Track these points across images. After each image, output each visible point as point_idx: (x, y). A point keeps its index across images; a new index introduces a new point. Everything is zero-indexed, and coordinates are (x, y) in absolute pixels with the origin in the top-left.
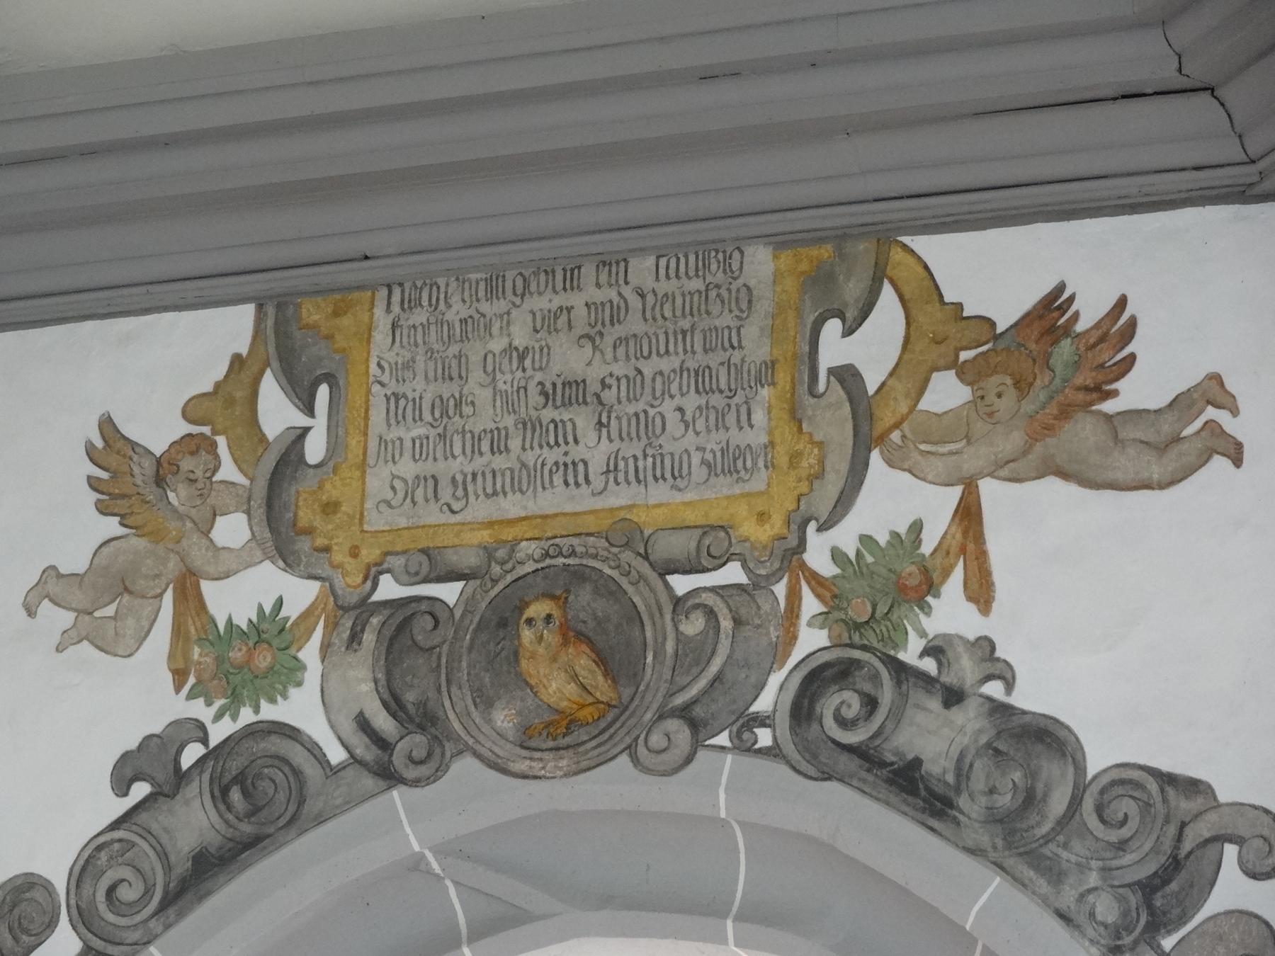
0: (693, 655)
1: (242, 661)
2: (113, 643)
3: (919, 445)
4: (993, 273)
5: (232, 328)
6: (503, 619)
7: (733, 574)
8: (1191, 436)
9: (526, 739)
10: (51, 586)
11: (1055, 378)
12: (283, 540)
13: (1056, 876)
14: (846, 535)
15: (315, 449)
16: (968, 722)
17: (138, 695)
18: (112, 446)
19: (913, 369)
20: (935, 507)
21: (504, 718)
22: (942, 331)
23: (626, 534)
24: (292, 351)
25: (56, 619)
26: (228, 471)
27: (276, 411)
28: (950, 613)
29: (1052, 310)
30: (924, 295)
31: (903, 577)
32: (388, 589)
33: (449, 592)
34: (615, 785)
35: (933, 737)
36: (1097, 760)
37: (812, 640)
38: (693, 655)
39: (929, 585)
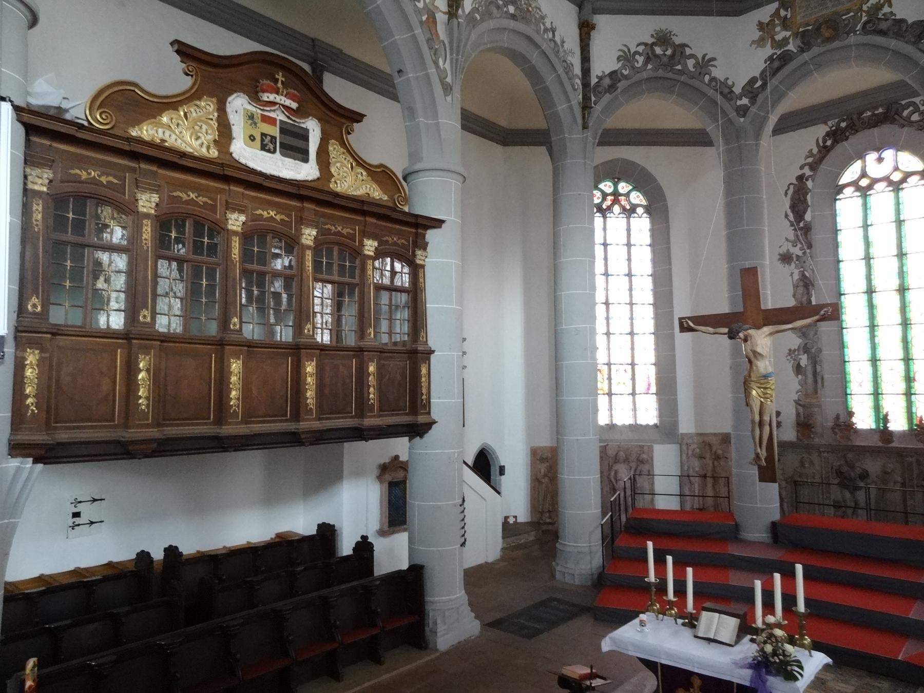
0: (846, 25)
2: (763, 46)
5: (776, 5)
6: (818, 29)
7: (852, 14)
9: (823, 42)
10: (753, 42)
12: (785, 27)
13: (904, 37)
14: (869, 4)
15: (789, 16)
16: (889, 23)
17: (768, 51)
21: (819, 41)
23: (835, 13)
24: (784, 5)
25: (754, 46)
26: (777, 22)
27: (783, 13)
28: (886, 9)
32: (801, 30)
33: (810, 28)
34: (837, 44)
35: (884, 26)
36: (910, 21)
37: (864, 19)
38: (846, 25)
39: (882, 6)
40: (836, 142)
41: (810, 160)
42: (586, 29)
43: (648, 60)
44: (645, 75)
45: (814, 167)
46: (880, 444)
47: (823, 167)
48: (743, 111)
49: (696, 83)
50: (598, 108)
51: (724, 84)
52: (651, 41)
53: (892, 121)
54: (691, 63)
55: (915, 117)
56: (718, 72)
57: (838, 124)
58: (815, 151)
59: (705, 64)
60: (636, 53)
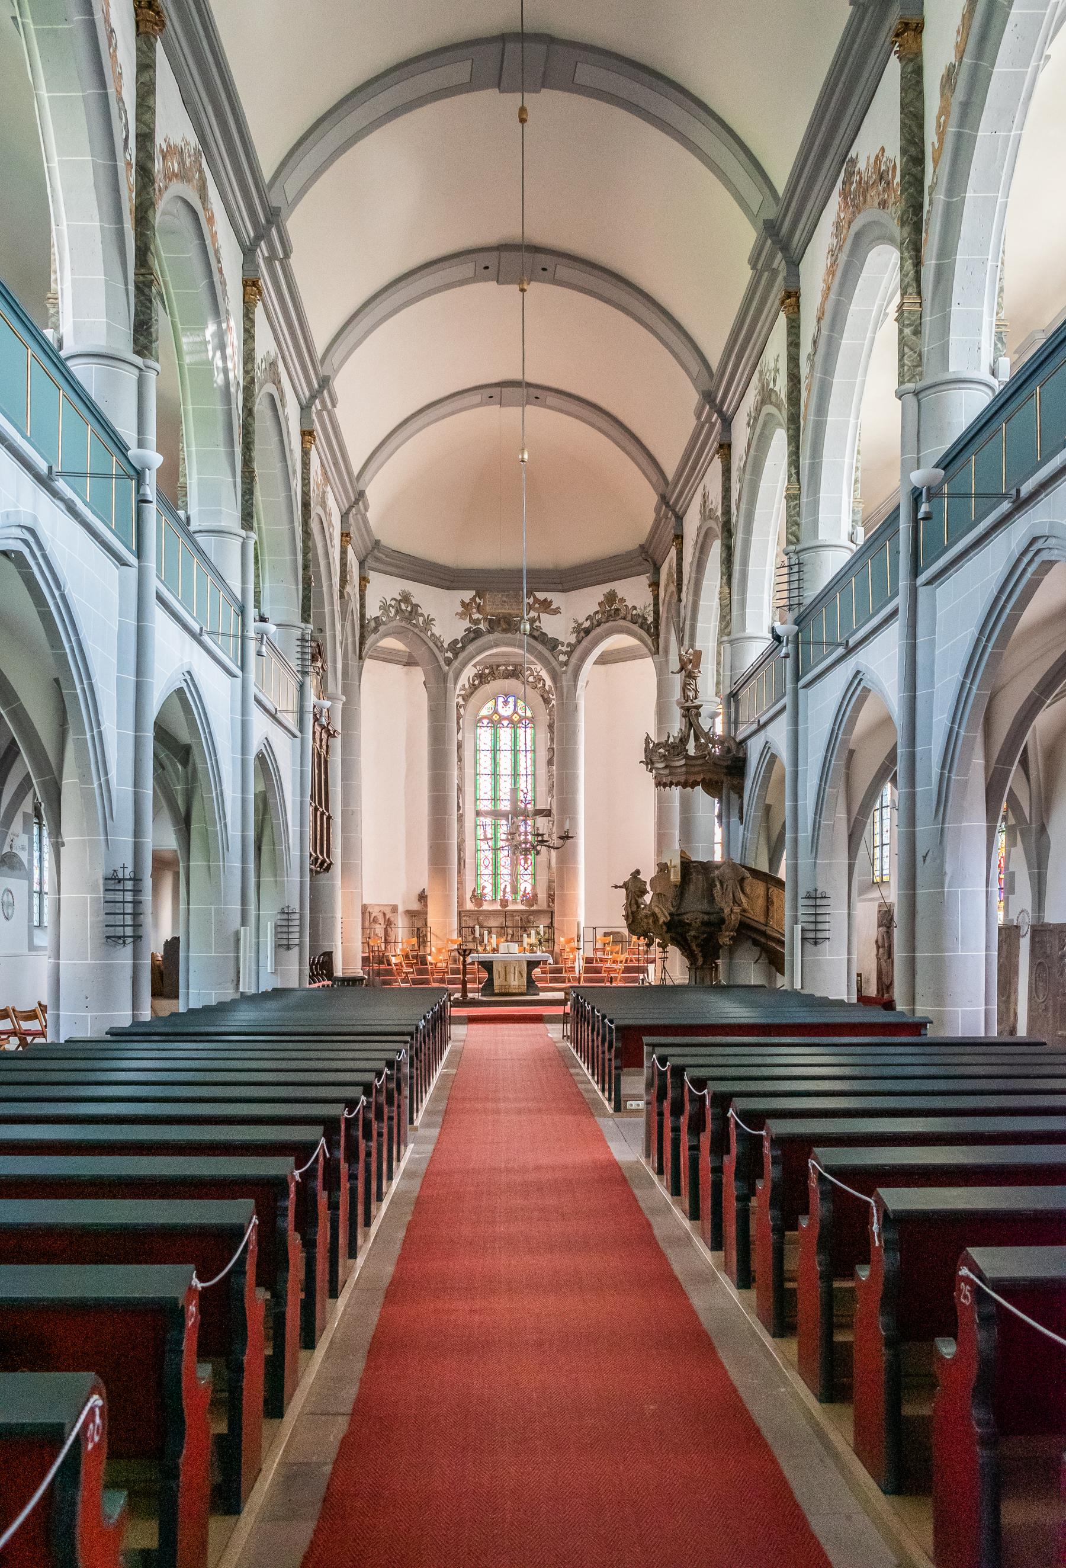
1: (476, 622)
3: (535, 610)
4: (541, 596)
5: (473, 593)
8: (557, 611)
10: (457, 614)
11: (546, 606)
12: (479, 611)
17: (466, 624)
18: (463, 602)
19: (534, 603)
20: (536, 615)
22: (536, 600)
23: (510, 614)
24: (479, 594)
28: (537, 623)
29: (545, 600)
30: (535, 597)
31: (532, 621)
34: (509, 635)
40: (481, 683)
41: (463, 692)
42: (364, 580)
43: (397, 612)
44: (395, 623)
45: (466, 698)
46: (499, 908)
47: (473, 700)
48: (449, 662)
49: (422, 635)
50: (368, 643)
51: (438, 639)
52: (399, 598)
53: (518, 678)
54: (421, 619)
55: (531, 679)
56: (436, 630)
57: (484, 669)
58: (467, 686)
59: (429, 621)
60: (390, 605)
